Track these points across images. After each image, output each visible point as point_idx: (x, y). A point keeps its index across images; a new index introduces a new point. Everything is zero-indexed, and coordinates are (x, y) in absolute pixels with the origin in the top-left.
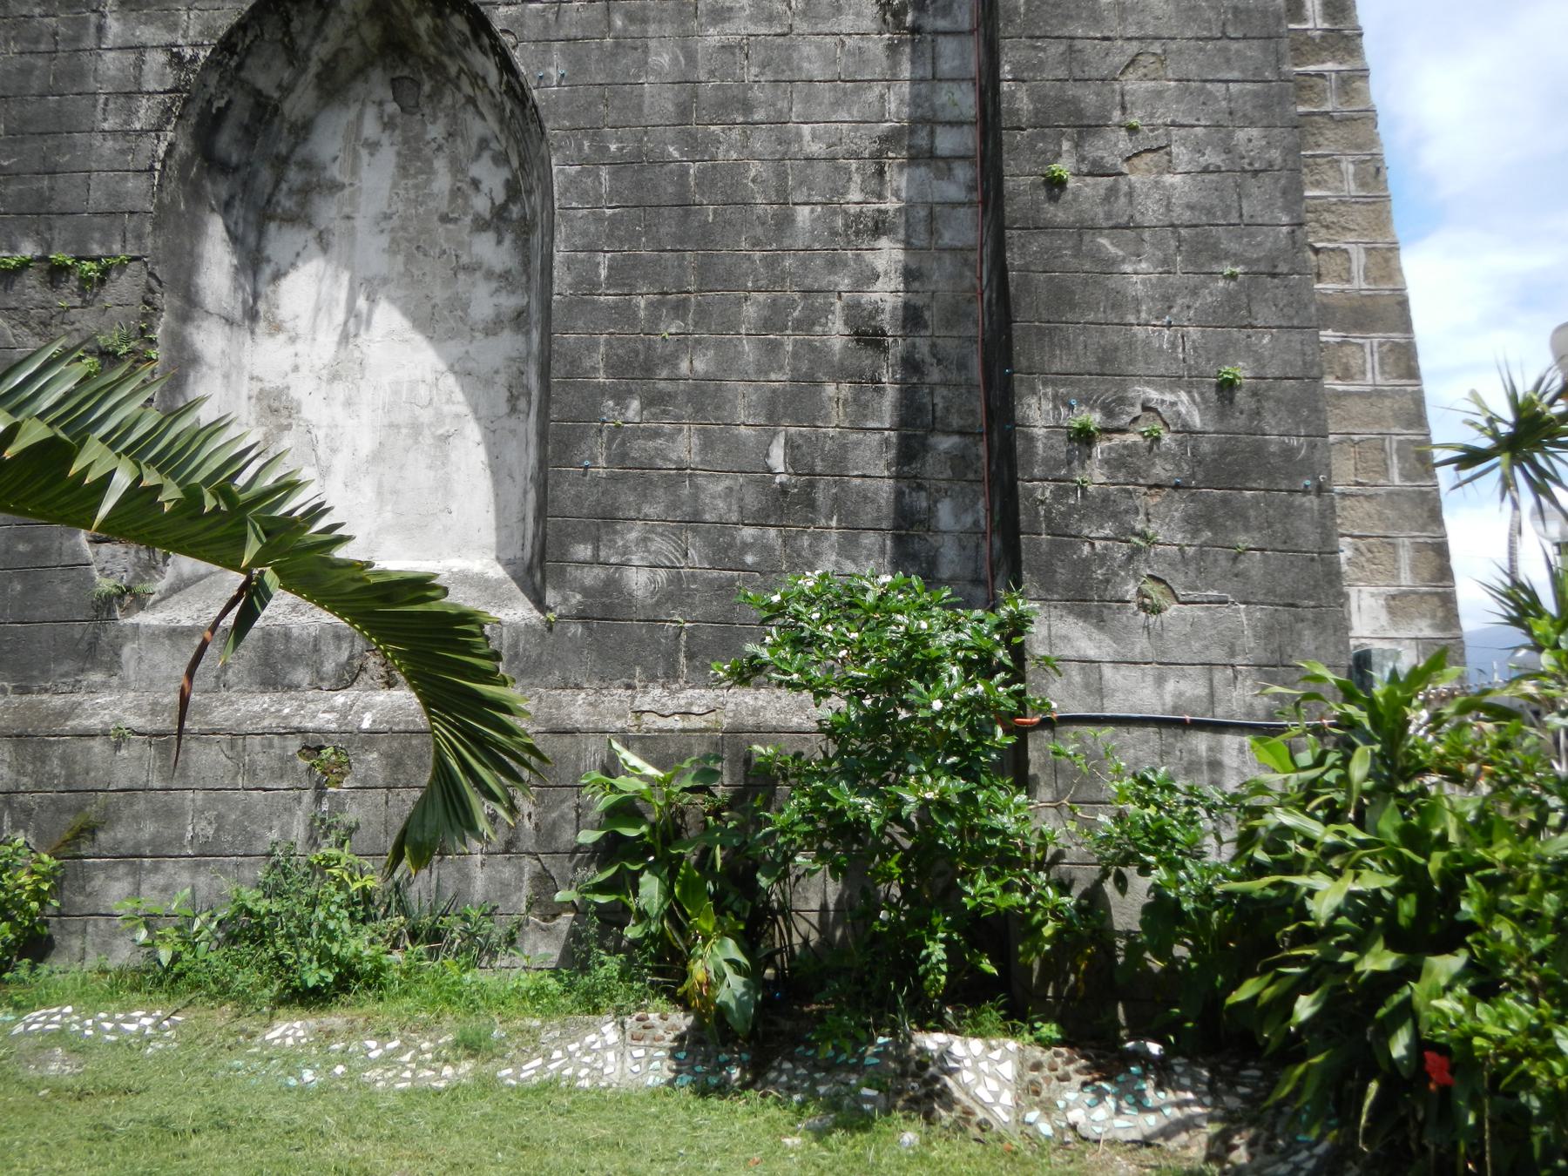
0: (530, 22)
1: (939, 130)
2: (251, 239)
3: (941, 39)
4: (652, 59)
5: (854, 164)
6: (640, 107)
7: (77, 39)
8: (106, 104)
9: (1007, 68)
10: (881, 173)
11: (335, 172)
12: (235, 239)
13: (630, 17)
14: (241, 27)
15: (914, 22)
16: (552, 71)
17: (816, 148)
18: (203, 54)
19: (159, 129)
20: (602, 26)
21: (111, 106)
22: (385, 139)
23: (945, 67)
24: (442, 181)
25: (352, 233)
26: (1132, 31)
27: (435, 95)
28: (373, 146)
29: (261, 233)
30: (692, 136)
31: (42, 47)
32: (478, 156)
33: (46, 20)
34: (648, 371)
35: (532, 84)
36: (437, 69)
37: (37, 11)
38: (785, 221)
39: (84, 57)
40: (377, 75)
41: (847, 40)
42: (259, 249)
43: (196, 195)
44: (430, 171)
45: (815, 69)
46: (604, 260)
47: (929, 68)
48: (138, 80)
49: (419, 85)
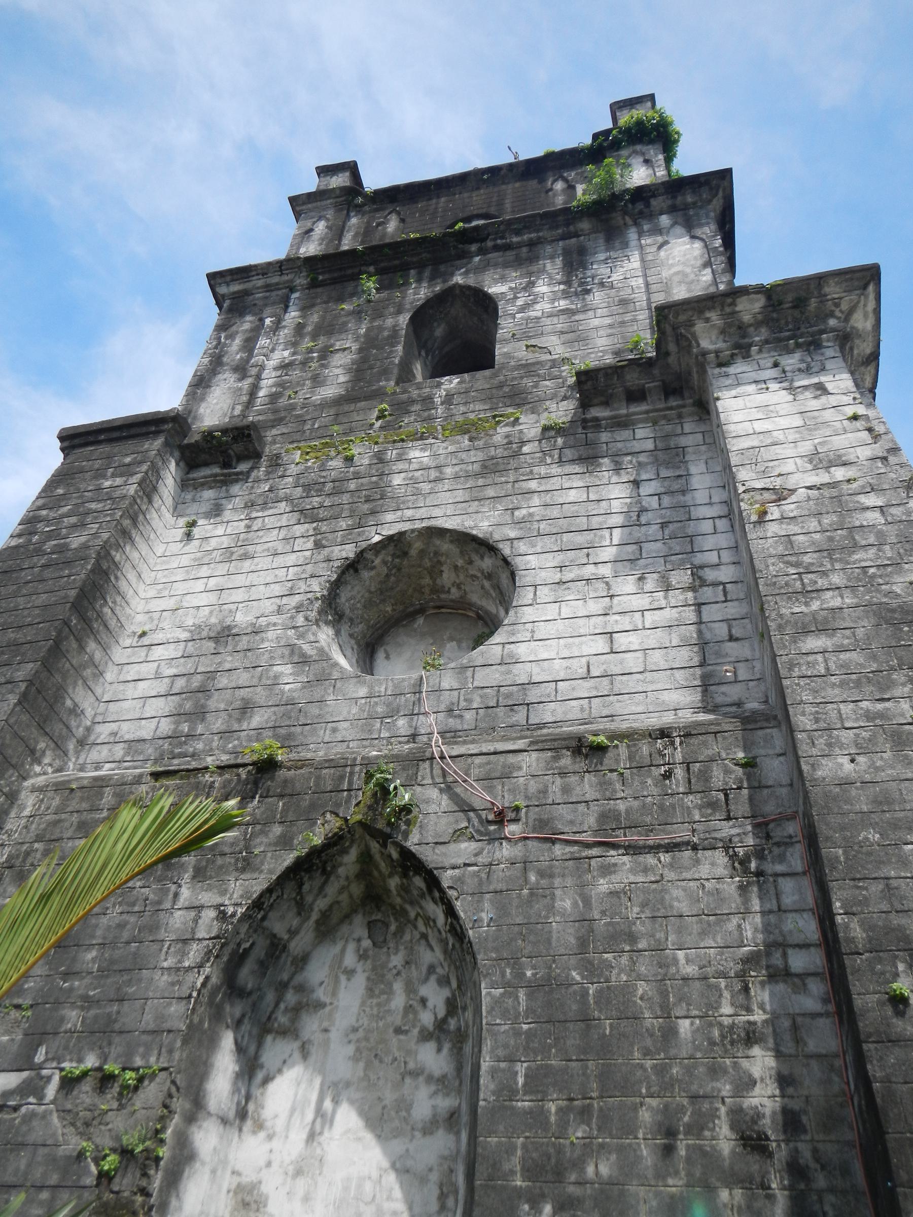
0: (469, 881)
1: (790, 951)
2: (252, 1049)
4: (558, 904)
5: (723, 983)
6: (549, 941)
7: (159, 902)
8: (169, 949)
9: (838, 904)
10: (746, 989)
11: (321, 994)
12: (240, 1049)
13: (541, 874)
14: (269, 891)
15: (757, 868)
17: (690, 970)
18: (240, 911)
19: (200, 966)
21: (172, 949)
23: (788, 900)
24: (399, 1001)
25: (326, 1043)
28: (350, 973)
29: (260, 1044)
30: (591, 963)
31: (136, 909)
32: (426, 980)
33: (143, 890)
34: (559, 1175)
35: (468, 925)
38: (669, 1033)
39: (162, 914)
40: (359, 920)
41: (707, 884)
42: (256, 1057)
43: (217, 1016)
44: (389, 992)
45: (684, 907)
46: (521, 1069)
47: (774, 902)
49: (387, 925)
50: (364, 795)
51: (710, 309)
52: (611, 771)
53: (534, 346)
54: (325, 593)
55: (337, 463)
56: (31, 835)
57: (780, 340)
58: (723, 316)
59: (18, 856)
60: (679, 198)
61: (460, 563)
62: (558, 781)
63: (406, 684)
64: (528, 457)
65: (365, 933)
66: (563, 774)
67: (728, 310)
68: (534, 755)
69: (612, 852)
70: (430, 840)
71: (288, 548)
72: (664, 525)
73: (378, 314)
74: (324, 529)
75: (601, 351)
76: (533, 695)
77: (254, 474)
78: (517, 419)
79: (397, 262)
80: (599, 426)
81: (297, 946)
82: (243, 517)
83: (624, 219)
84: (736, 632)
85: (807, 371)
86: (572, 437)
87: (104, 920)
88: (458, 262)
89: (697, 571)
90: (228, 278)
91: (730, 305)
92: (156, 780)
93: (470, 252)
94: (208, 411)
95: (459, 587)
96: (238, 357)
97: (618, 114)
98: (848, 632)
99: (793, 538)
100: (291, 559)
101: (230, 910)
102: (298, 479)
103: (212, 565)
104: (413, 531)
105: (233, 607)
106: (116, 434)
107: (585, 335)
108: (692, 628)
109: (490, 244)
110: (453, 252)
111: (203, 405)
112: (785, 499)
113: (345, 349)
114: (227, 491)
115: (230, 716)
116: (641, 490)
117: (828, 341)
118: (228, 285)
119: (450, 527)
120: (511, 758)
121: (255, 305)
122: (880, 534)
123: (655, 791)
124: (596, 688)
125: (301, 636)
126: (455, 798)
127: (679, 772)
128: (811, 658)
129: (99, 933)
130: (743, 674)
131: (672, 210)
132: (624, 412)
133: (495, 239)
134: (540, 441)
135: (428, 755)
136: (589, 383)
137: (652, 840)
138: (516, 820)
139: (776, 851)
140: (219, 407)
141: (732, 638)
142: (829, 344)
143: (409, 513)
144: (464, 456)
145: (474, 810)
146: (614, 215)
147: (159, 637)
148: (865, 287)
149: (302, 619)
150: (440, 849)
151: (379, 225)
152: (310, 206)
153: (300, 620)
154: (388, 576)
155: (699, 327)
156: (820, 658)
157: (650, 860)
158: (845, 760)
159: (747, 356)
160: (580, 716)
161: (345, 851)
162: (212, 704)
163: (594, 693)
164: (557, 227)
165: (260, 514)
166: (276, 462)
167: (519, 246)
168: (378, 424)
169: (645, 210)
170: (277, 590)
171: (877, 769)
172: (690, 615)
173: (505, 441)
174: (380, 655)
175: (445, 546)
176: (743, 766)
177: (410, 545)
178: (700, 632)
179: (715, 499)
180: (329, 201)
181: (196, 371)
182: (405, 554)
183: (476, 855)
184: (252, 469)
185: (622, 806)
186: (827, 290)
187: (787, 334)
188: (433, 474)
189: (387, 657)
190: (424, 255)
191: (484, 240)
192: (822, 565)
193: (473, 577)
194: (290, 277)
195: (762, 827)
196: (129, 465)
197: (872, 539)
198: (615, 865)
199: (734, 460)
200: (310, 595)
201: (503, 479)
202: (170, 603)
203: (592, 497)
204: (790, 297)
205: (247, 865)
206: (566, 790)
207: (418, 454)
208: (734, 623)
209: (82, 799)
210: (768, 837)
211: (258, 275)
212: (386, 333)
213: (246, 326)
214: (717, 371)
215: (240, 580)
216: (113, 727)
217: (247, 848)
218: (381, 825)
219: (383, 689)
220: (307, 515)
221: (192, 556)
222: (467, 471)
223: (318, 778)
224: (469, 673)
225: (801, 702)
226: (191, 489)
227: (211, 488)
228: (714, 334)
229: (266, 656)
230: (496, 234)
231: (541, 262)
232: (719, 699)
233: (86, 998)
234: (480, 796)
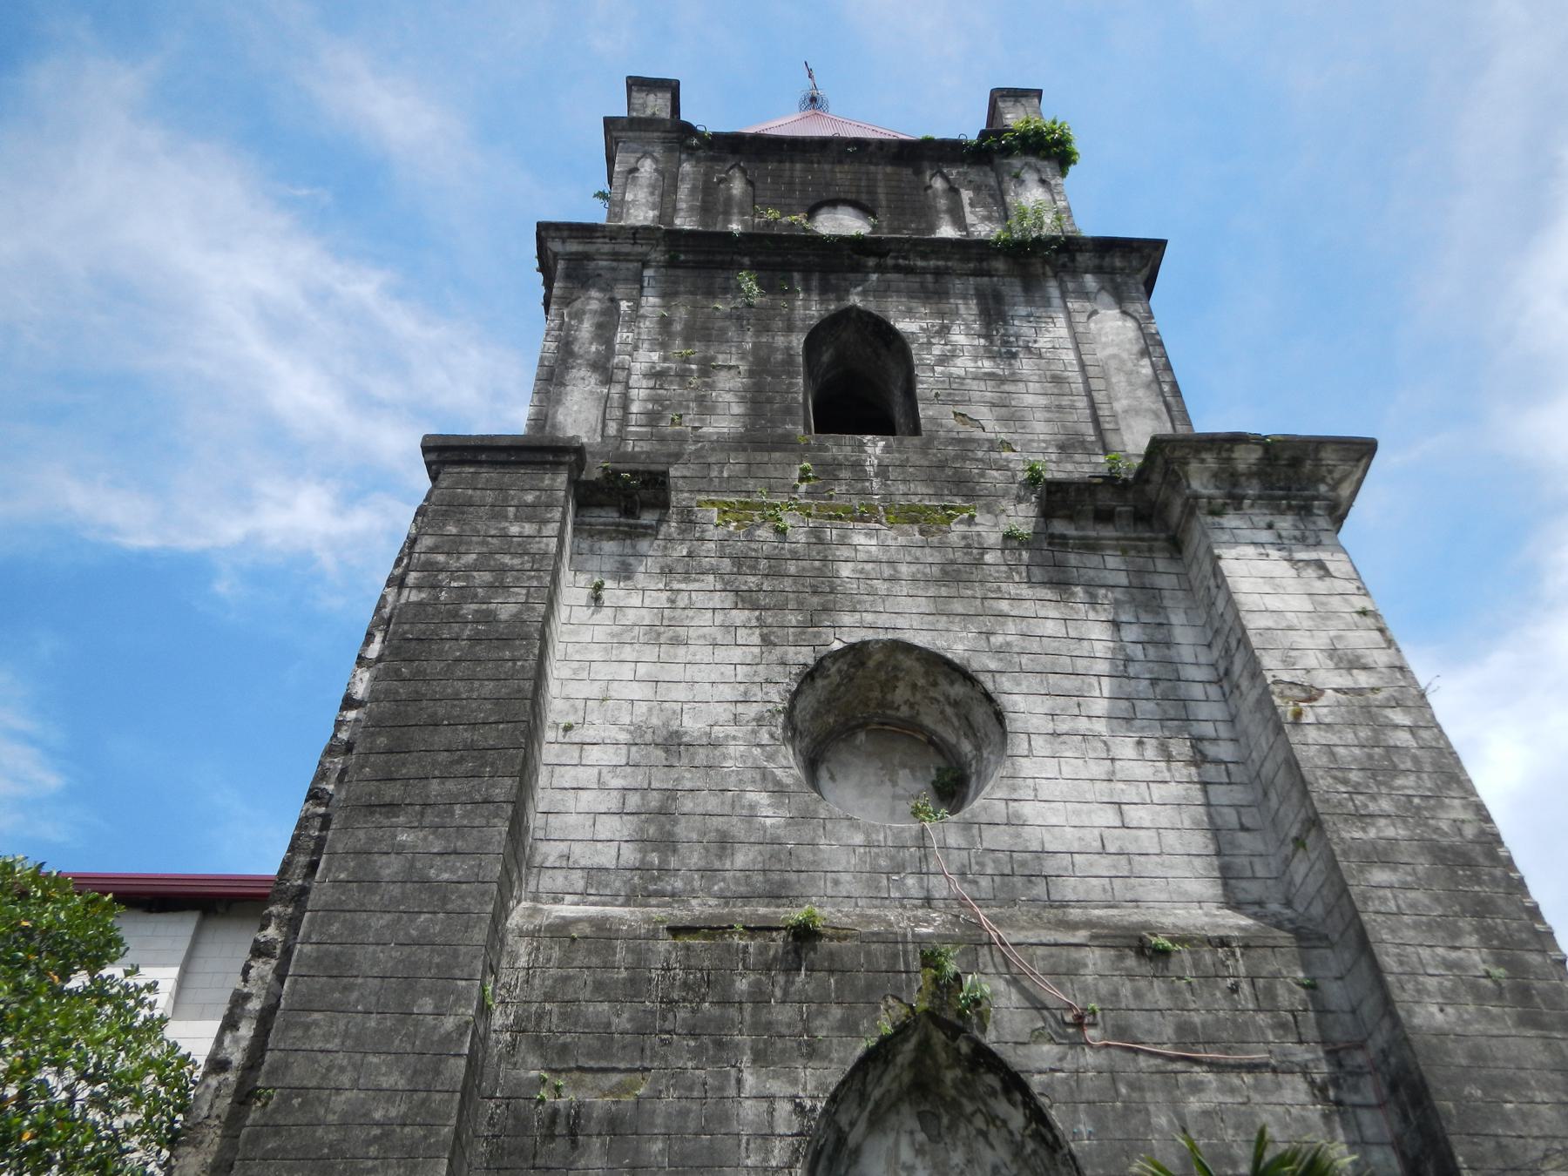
0: (1058, 1088)
3: (1360, 1112)
4: (1154, 1120)
7: (721, 1088)
8: (748, 1144)
9: (1460, 1159)
13: (1132, 1086)
15: (1336, 1096)
16: (1081, 1127)
18: (820, 1105)
20: (1112, 1093)
21: (752, 1145)
22: (918, 1163)
26: (1536, 1131)
27: (952, 1127)
31: (695, 1094)
33: (697, 1072)
35: (1069, 1138)
36: (954, 1106)
37: (690, 1064)
39: (728, 1103)
40: (905, 1109)
41: (1292, 1110)
47: (1356, 1133)
48: (771, 1125)
49: (938, 1118)
50: (923, 979)
52: (1180, 978)
53: (964, 415)
54: (787, 705)
55: (765, 533)
56: (537, 994)
57: (1272, 498)
58: (1219, 460)
59: (528, 1018)
61: (921, 682)
62: (1128, 985)
63: (907, 834)
64: (992, 568)
65: (916, 1125)
66: (1131, 976)
67: (1224, 455)
68: (1098, 952)
69: (1197, 1069)
70: (1008, 1038)
71: (729, 639)
72: (1154, 681)
73: (764, 328)
74: (770, 620)
75: (1044, 441)
76: (1050, 866)
77: (664, 528)
78: (972, 517)
80: (1065, 545)
81: (853, 1139)
82: (661, 586)
83: (1044, 268)
84: (1247, 821)
85: (1302, 540)
86: (1038, 552)
87: (660, 1106)
88: (851, 276)
89: (1197, 740)
90: (566, 233)
91: (1227, 450)
92: (675, 937)
93: (866, 266)
94: (570, 420)
95: (912, 706)
96: (593, 348)
97: (1001, 104)
98: (1409, 868)
99: (1336, 749)
100: (737, 654)
101: (808, 1104)
102: (722, 546)
103: (636, 646)
104: (877, 641)
105: (677, 707)
106: (502, 457)
107: (1019, 414)
108: (1202, 810)
109: (890, 262)
110: (847, 262)
111: (561, 410)
112: (1315, 700)
113: (730, 368)
114: (634, 547)
115: (707, 850)
116: (1123, 633)
117: (1319, 508)
118: (564, 242)
119: (920, 644)
120: (1076, 954)
121: (599, 275)
122: (1415, 759)
123: (1226, 1005)
124: (1114, 867)
125: (770, 758)
126: (1023, 991)
127: (1245, 987)
128: (1381, 892)
129: (659, 1121)
130: (1260, 872)
131: (1098, 271)
132: (1093, 534)
133: (896, 258)
134: (1003, 550)
135: (985, 939)
136: (1059, 495)
137: (1232, 1058)
138: (1094, 1025)
139: (1350, 1080)
140: (582, 416)
141: (1243, 828)
142: (1320, 512)
143: (869, 618)
144: (918, 552)
145: (1047, 1008)
146: (1034, 260)
147: (589, 734)
148: (1359, 460)
149: (767, 736)
150: (1021, 1050)
151: (721, 181)
153: (765, 738)
154: (839, 685)
155: (1194, 466)
156: (1388, 893)
157: (1234, 1079)
158: (1434, 1009)
160: (1103, 898)
161: (906, 1040)
162: (682, 830)
163: (1113, 873)
164: (969, 260)
165: (683, 586)
166: (688, 519)
167: (924, 271)
168: (803, 487)
169: (1069, 264)
170: (728, 693)
171: (1467, 1023)
172: (1196, 793)
173: (963, 543)
174: (823, 774)
175: (907, 662)
176: (1304, 986)
177: (870, 655)
178: (1210, 816)
179: (1202, 659)
180: (656, 134)
181: (542, 359)
182: (863, 664)
183: (1061, 1060)
184: (660, 521)
185: (1196, 1019)
186: (1323, 455)
187: (1281, 493)
188: (887, 571)
189: (832, 778)
190: (811, 258)
191: (882, 255)
192: (1368, 786)
193: (934, 700)
194: (644, 249)
195: (1334, 1055)
196: (533, 506)
197: (1409, 765)
198: (1201, 1082)
199: (1255, 641)
200: (770, 706)
201: (969, 592)
202: (594, 690)
203: (1072, 634)
204: (1286, 455)
205: (812, 1052)
206: (1138, 995)
207: (863, 540)
208: (1242, 810)
209: (589, 952)
210: (1340, 1065)
211: (604, 237)
212: (779, 357)
213: (594, 305)
214: (1209, 519)
215: (676, 672)
216: (562, 847)
217: (807, 1030)
218: (950, 1015)
219: (881, 838)
220: (745, 599)
221: (608, 629)
222: (925, 574)
223: (868, 954)
224: (975, 830)
225: (1382, 941)
226: (585, 535)
227: (612, 539)
228: (1206, 475)
229: (733, 778)
230: (899, 251)
231: (952, 301)
232: (1241, 896)
234: (1053, 994)
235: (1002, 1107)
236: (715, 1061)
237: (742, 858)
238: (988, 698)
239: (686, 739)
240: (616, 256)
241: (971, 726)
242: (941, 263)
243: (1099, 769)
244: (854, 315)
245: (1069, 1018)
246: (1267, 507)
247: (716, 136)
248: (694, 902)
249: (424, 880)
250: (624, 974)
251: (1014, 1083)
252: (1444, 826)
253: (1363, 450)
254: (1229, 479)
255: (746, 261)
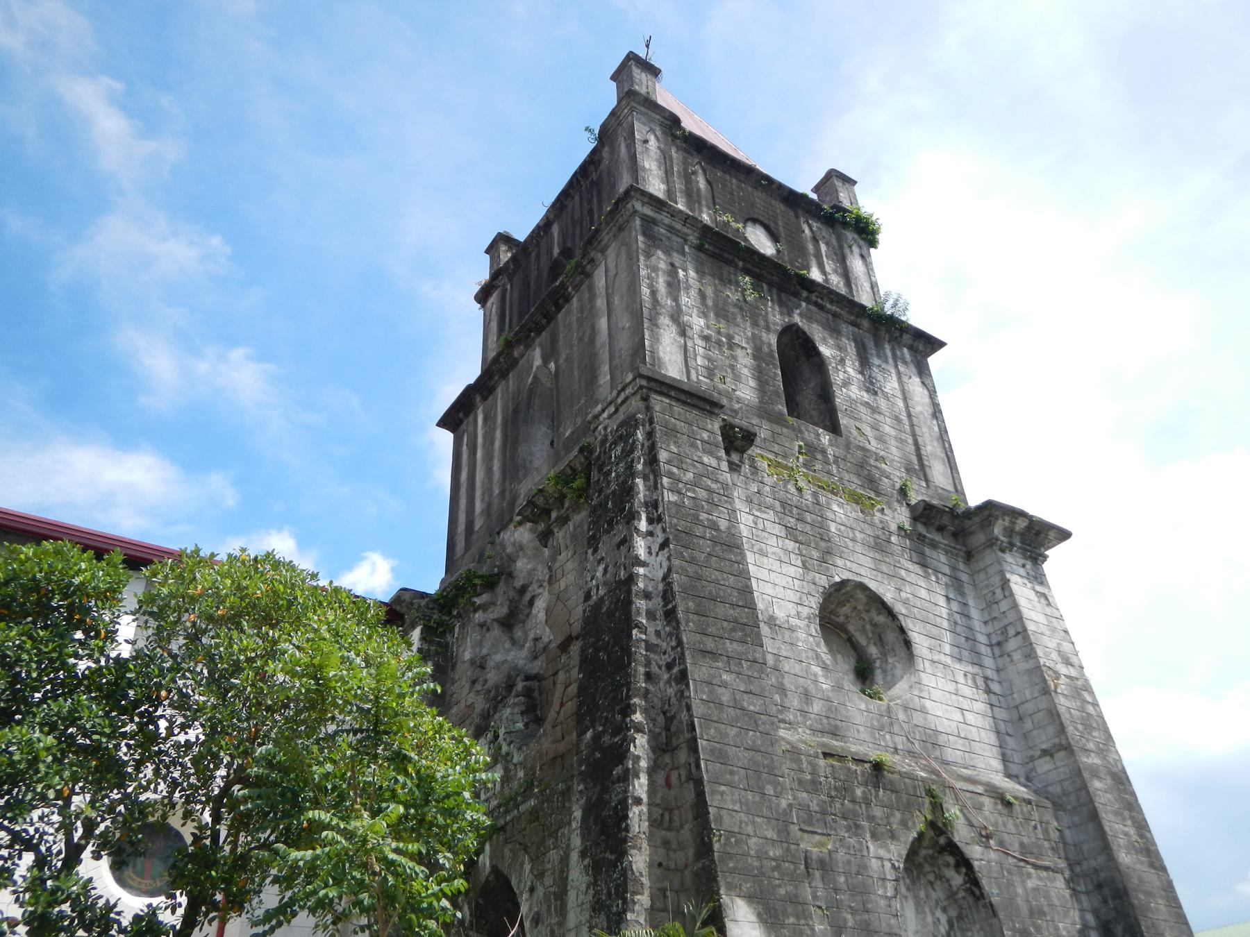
24: (929, 919)
51: (1008, 515)
60: (916, 343)
61: (860, 607)
79: (758, 271)
80: (924, 541)
90: (646, 200)
106: (683, 397)
113: (743, 348)
129: (840, 865)
131: (911, 348)
132: (937, 539)
141: (1009, 735)
150: (969, 847)
152: (642, 108)
159: (1011, 551)
180: (657, 117)
194: (688, 231)
195: (1071, 867)
223: (905, 783)
233: (851, 908)
235: (950, 873)
236: (857, 835)
237: (817, 707)
238: (902, 630)
239: (778, 622)
240: (671, 229)
241: (881, 639)
242: (838, 310)
243: (951, 687)
244: (794, 328)
245: (984, 833)
246: (1022, 554)
247: (691, 134)
248: (800, 730)
249: (743, 709)
250: (809, 777)
251: (964, 863)
252: (1111, 760)
253: (1064, 535)
254: (1010, 532)
255: (741, 264)
